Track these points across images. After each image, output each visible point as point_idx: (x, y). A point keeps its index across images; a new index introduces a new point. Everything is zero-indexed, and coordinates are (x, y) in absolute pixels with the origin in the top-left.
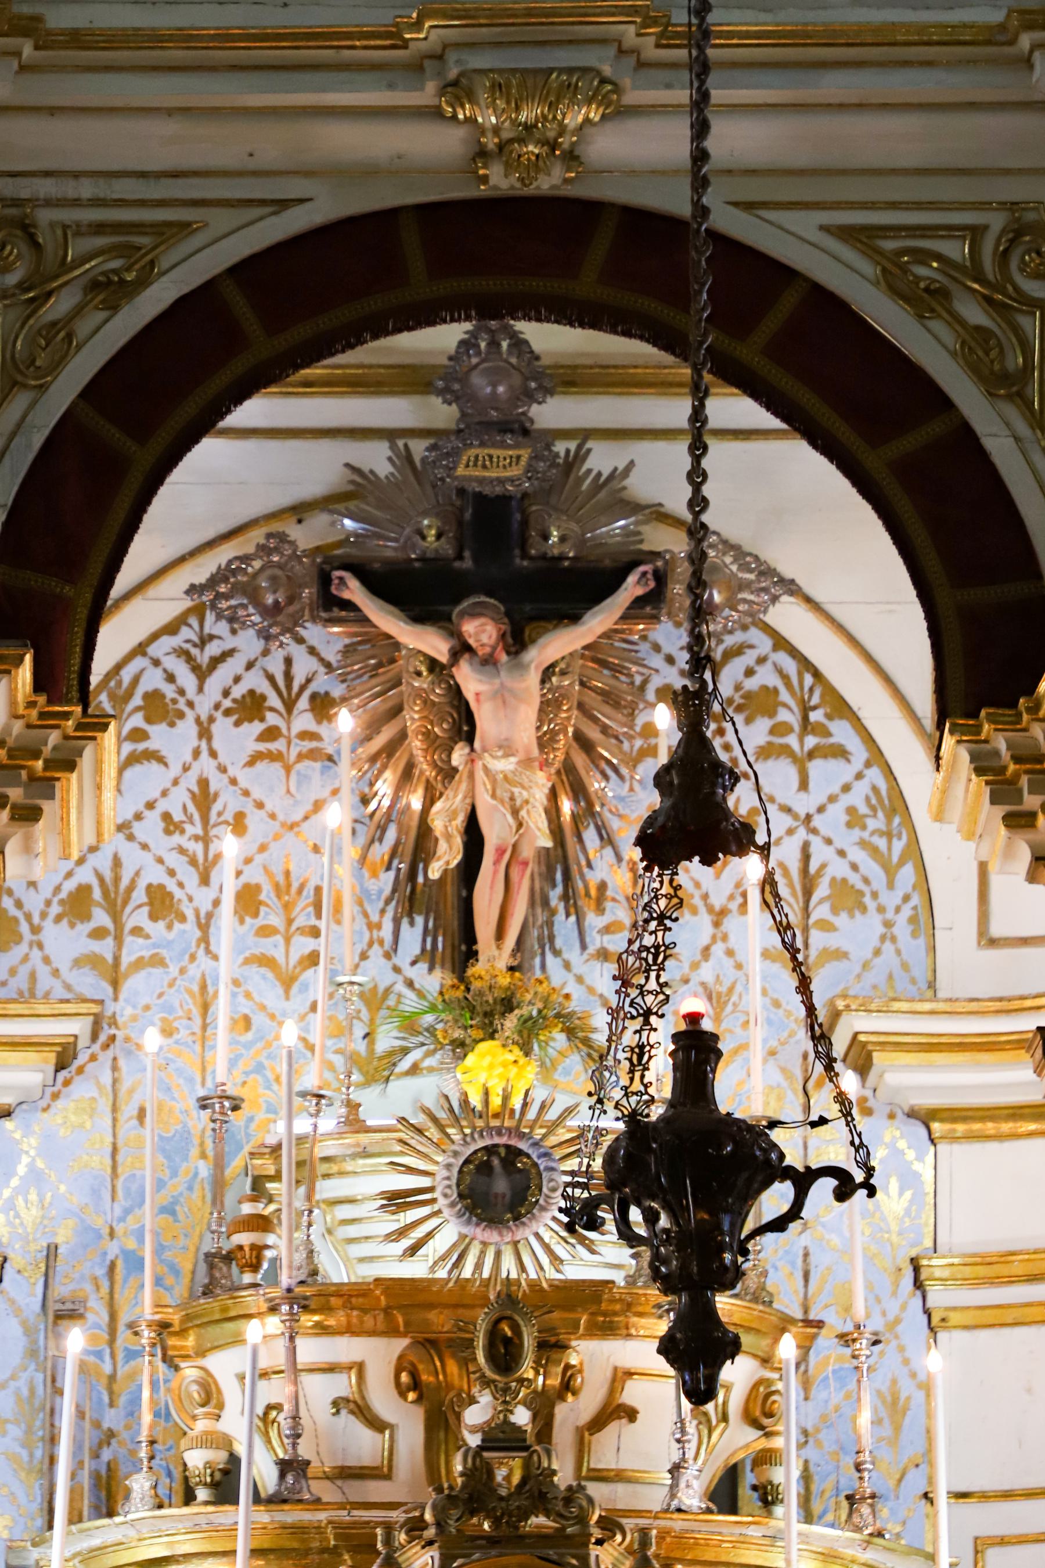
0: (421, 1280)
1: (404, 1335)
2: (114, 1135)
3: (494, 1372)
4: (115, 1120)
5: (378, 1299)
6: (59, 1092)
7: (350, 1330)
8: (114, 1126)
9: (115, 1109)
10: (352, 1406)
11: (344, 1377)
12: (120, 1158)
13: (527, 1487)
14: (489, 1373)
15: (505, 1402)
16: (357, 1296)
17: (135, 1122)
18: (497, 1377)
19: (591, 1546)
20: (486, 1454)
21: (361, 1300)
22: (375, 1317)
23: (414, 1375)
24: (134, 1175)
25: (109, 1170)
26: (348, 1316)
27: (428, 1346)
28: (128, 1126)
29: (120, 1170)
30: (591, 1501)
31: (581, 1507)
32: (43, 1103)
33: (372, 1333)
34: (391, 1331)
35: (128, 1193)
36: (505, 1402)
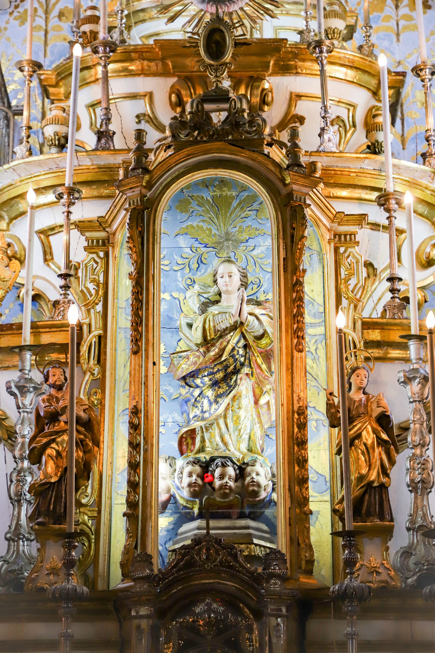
0: (180, 40)
1: (173, 75)
2: (46, 26)
3: (210, 60)
4: (47, 18)
5: (158, 53)
6: (19, 5)
7: (143, 73)
8: (46, 21)
9: (47, 12)
10: (147, 118)
11: (142, 101)
12: (49, 36)
13: (229, 120)
14: (208, 61)
15: (216, 76)
16: (146, 52)
17: (57, 19)
18: (212, 62)
19: (265, 146)
20: (207, 107)
21: (148, 54)
22: (157, 65)
23: (179, 96)
24: (56, 45)
25: (43, 42)
26: (142, 64)
27: (186, 80)
28: (54, 21)
29: (48, 42)
30: (264, 121)
31: (259, 125)
32: (10, 10)
33: (155, 74)
34: (165, 74)
35: (52, 53)
36: (216, 76)
